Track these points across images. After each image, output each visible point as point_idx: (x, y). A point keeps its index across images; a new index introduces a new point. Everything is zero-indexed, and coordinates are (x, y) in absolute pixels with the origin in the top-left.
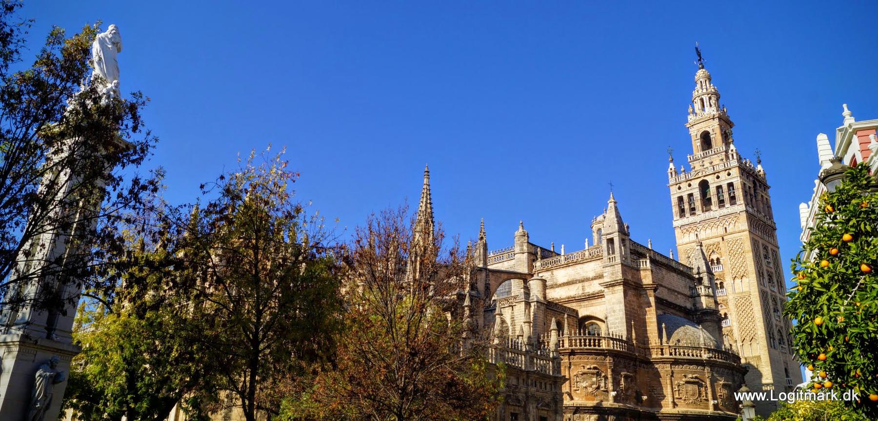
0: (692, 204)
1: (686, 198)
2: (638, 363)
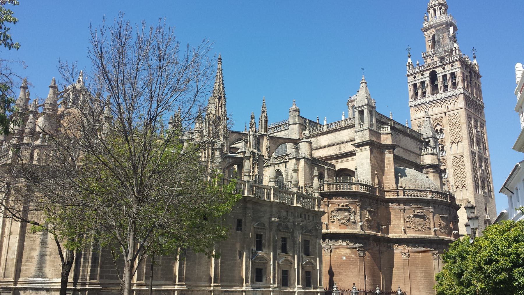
0: (424, 89)
2: (379, 202)
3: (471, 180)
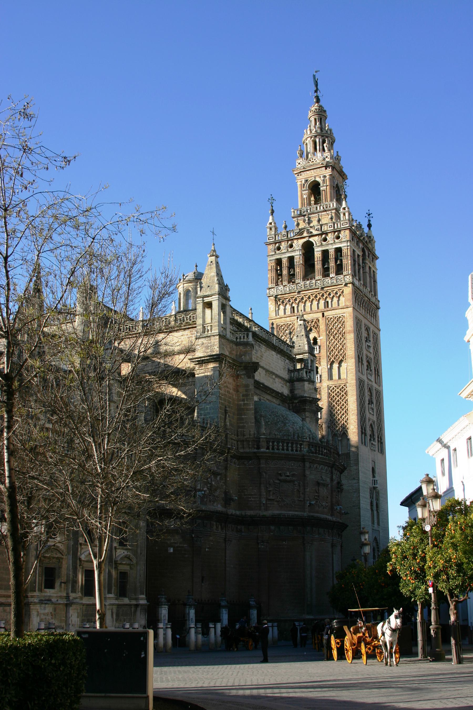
1: (285, 262)
3: (356, 424)
